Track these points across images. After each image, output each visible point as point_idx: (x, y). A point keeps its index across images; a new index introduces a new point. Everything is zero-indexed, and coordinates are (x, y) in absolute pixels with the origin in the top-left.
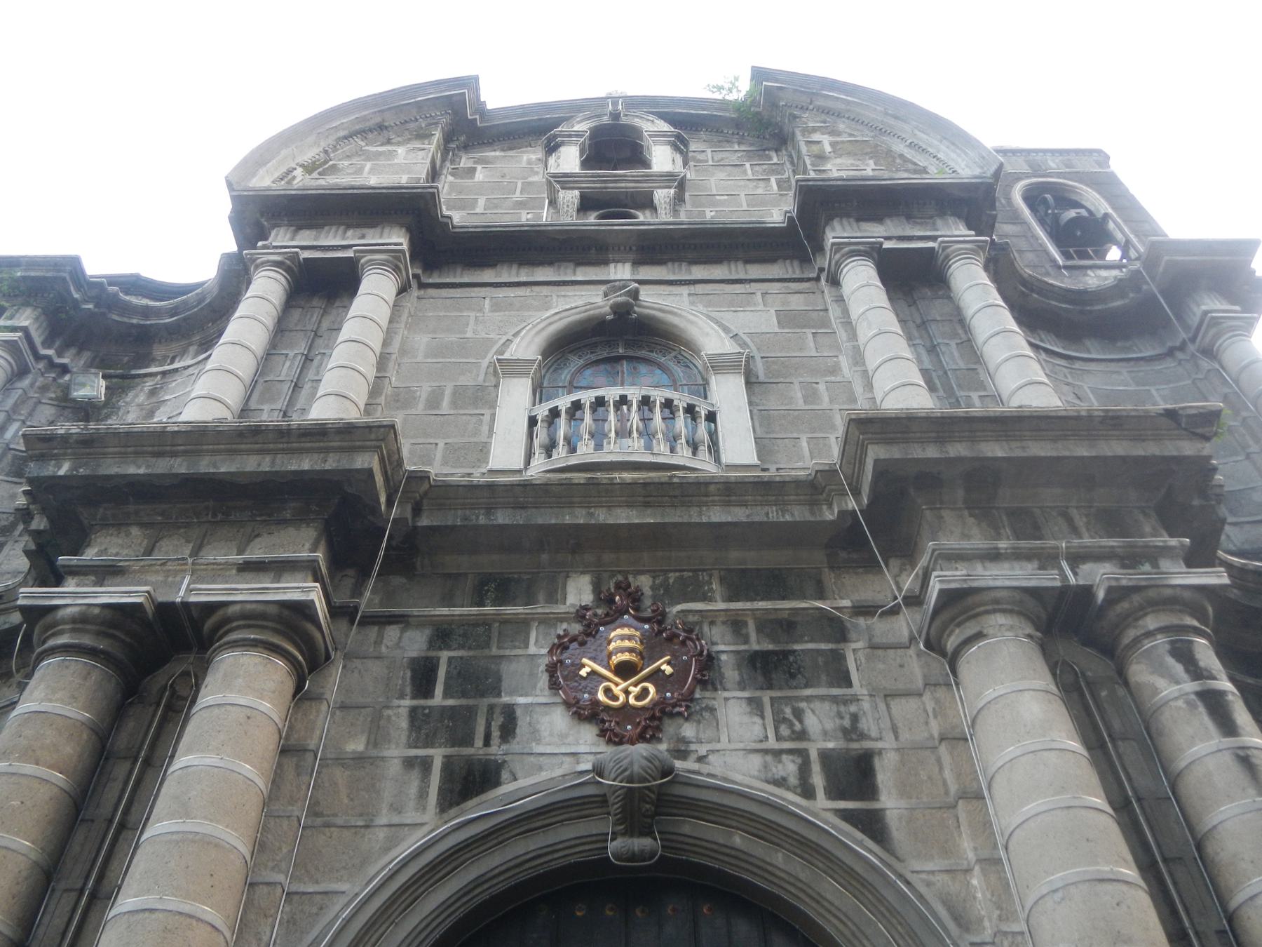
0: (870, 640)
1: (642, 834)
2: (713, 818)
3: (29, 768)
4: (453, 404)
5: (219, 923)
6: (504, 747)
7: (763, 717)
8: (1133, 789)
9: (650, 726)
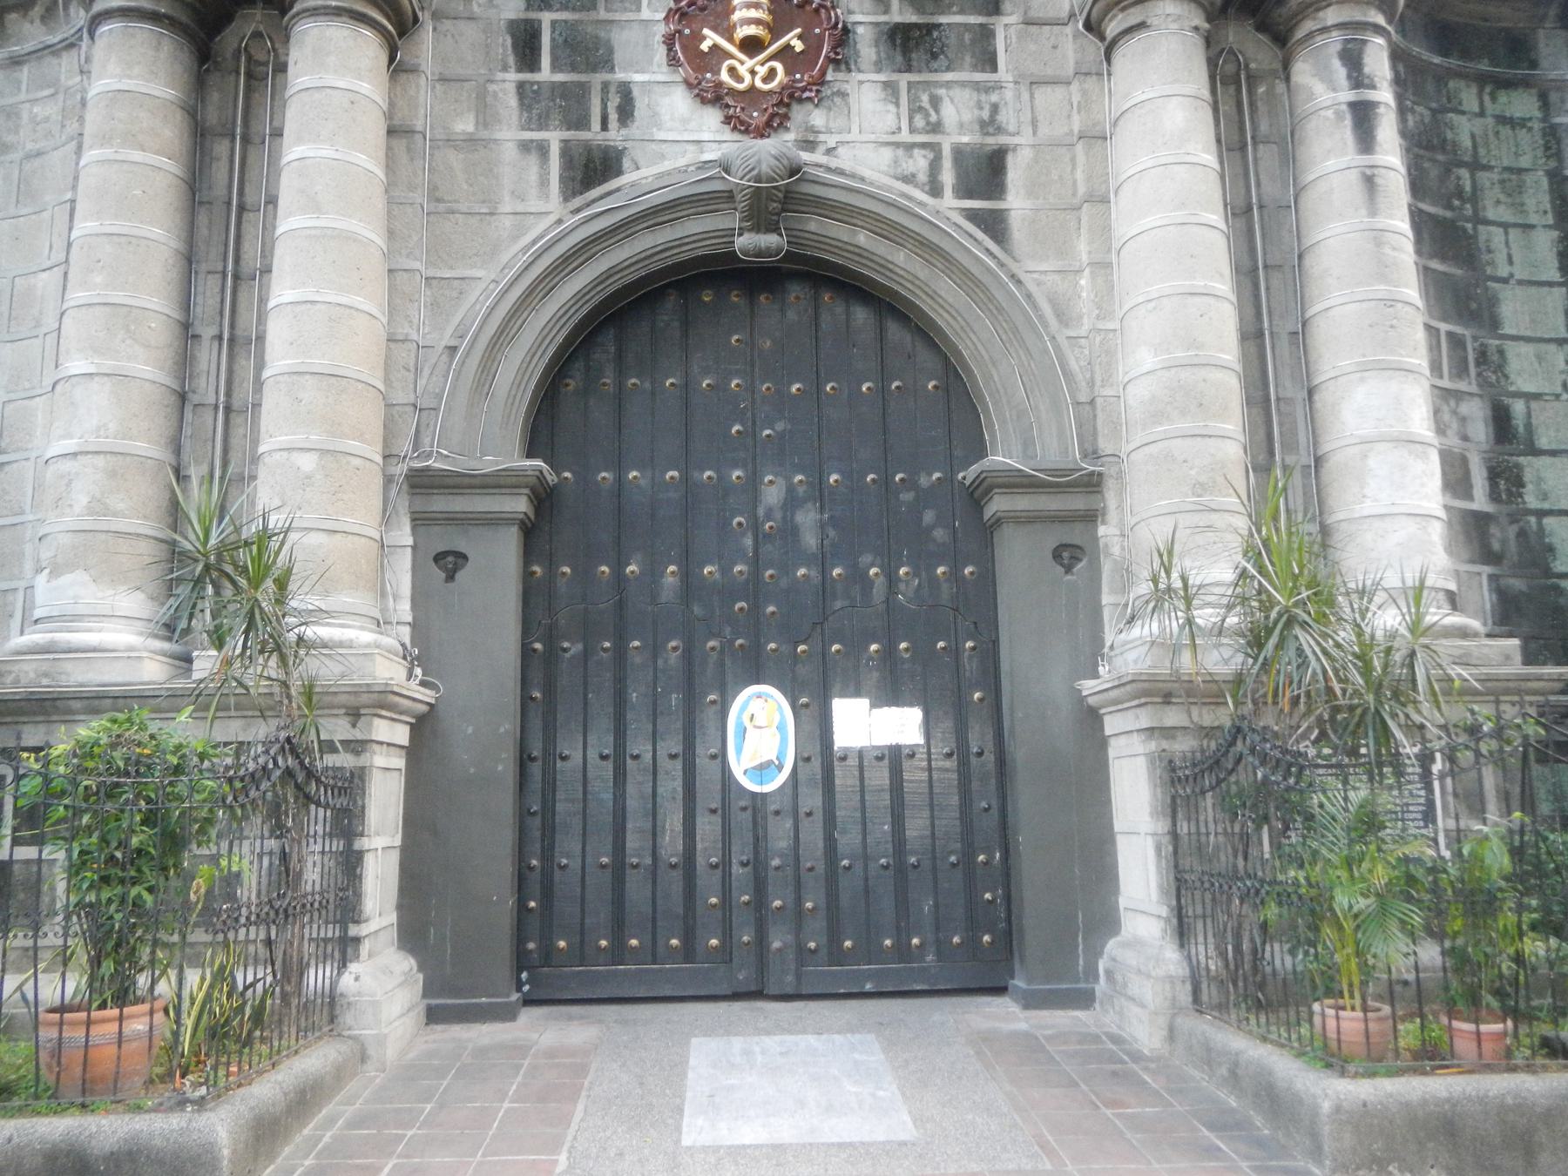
0: (1025, 13)
1: (768, 230)
2: (839, 217)
3: (137, 156)
5: (375, 312)
6: (624, 132)
7: (897, 105)
8: (1259, 196)
9: (777, 114)
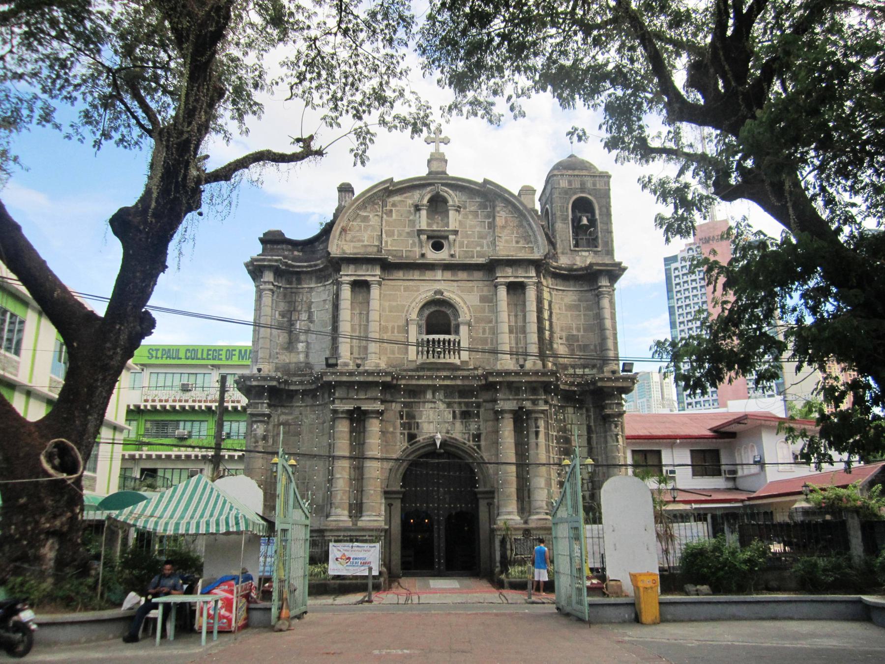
4: (398, 333)
